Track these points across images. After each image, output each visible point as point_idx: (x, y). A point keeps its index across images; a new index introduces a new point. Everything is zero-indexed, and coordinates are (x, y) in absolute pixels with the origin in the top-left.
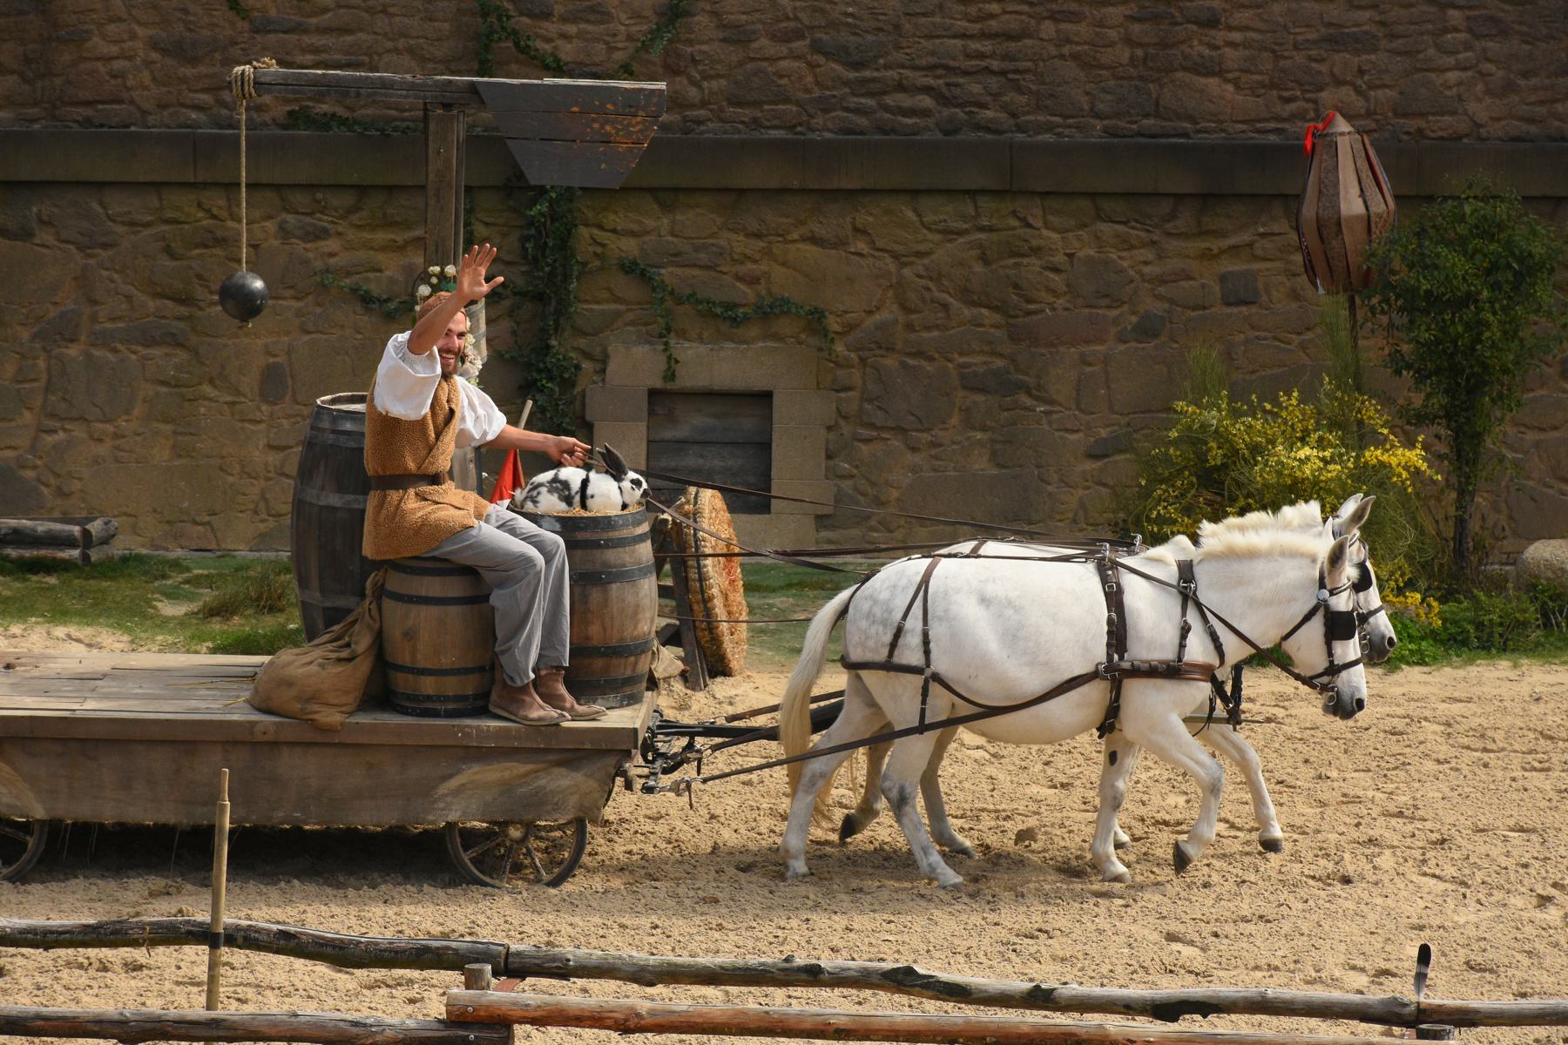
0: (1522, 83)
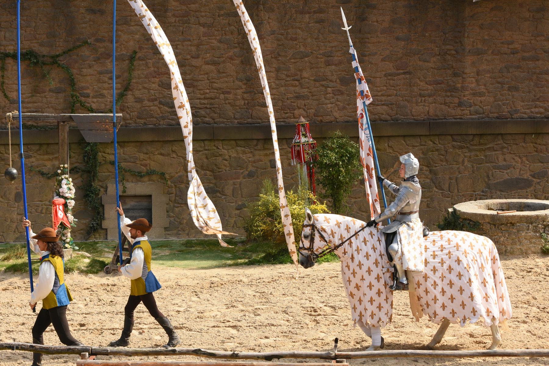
0: (347, 107)
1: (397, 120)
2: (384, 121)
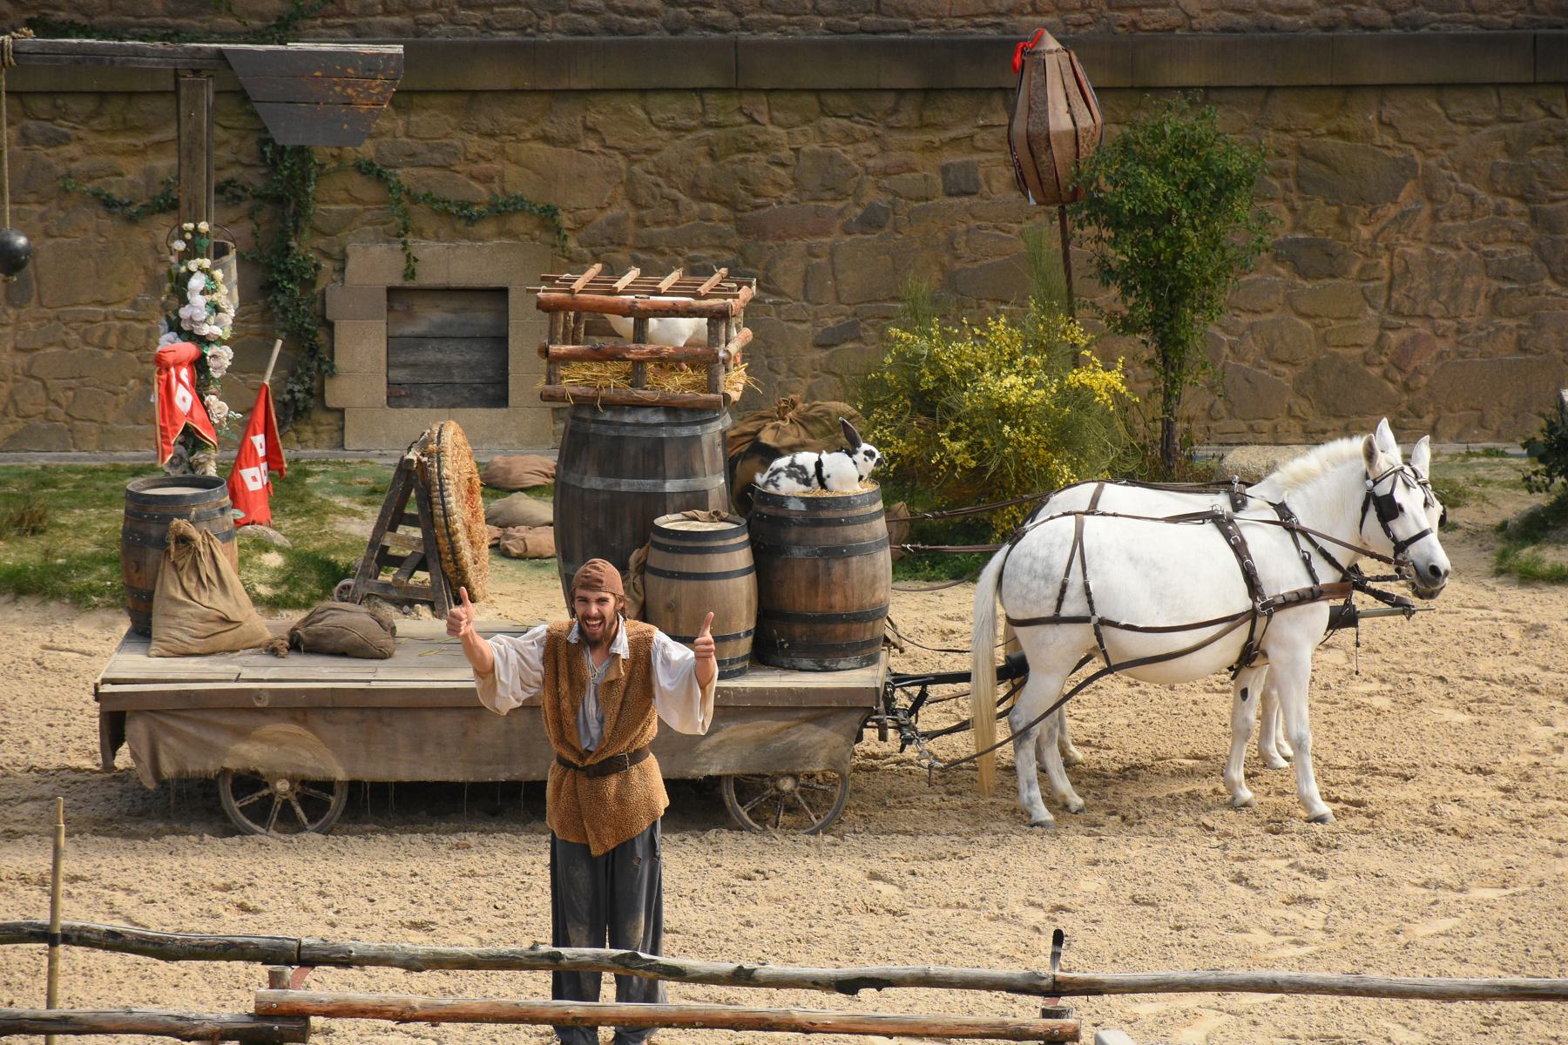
1: (1415, 27)
2: (1364, 28)
